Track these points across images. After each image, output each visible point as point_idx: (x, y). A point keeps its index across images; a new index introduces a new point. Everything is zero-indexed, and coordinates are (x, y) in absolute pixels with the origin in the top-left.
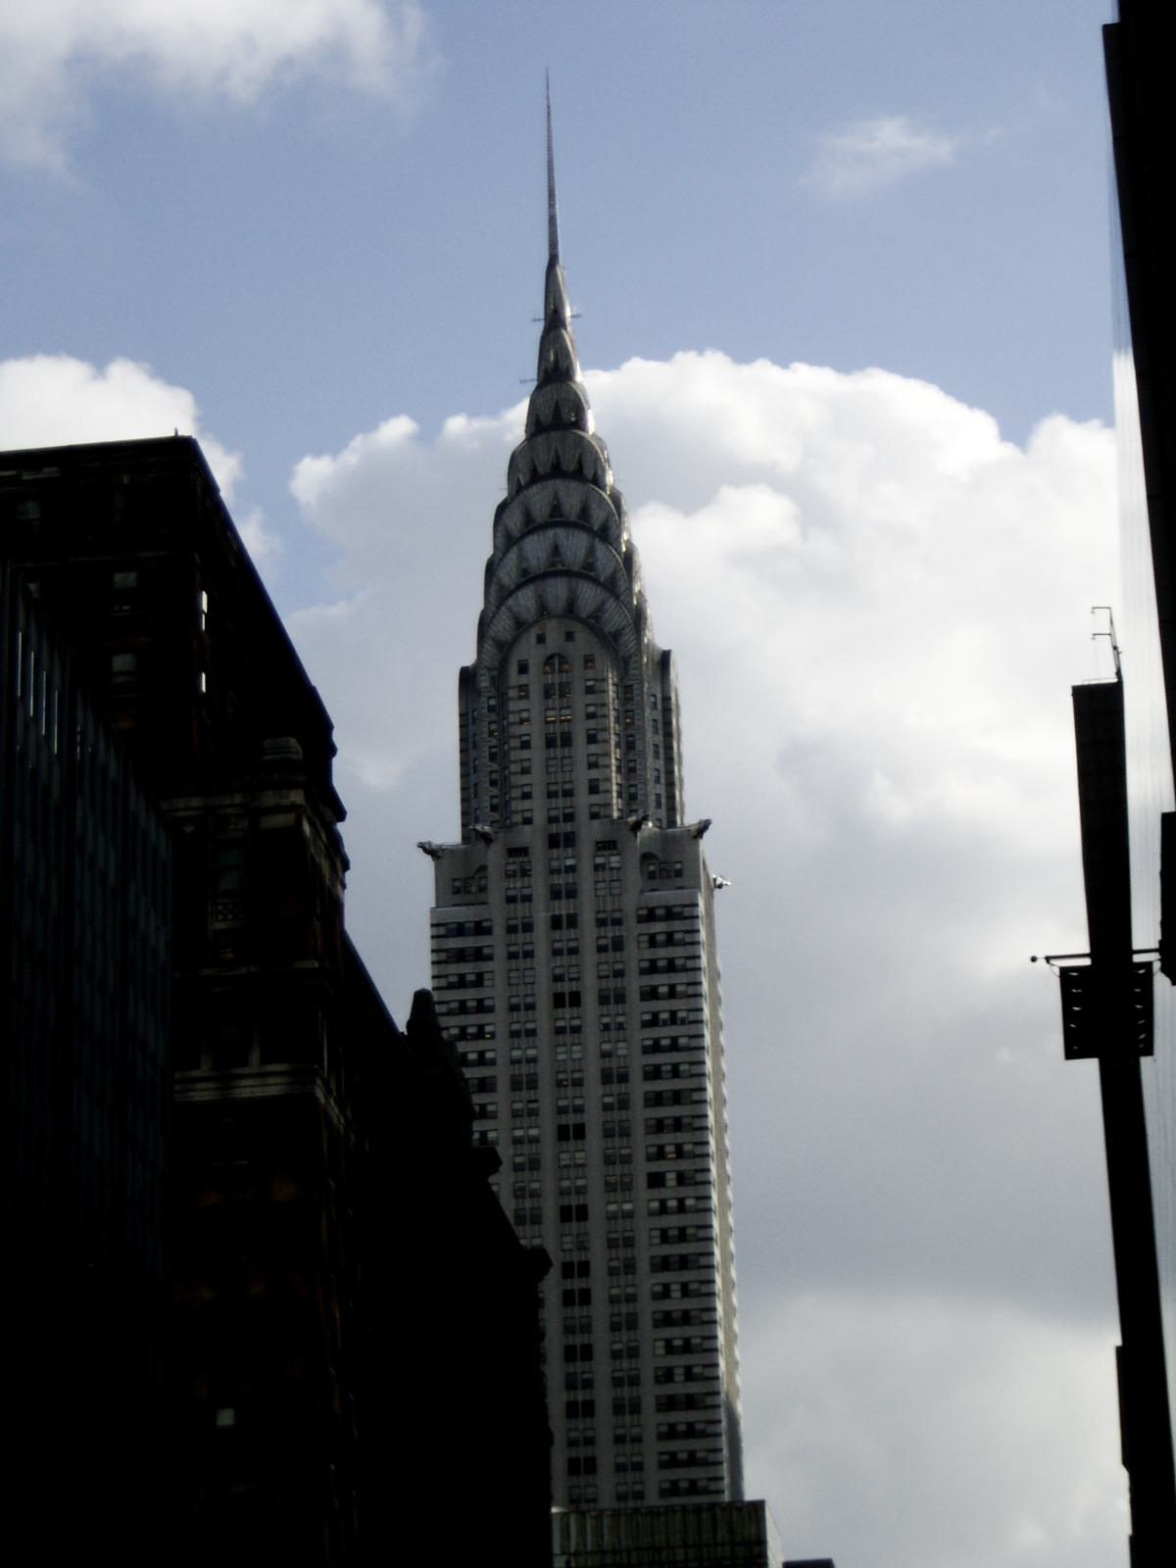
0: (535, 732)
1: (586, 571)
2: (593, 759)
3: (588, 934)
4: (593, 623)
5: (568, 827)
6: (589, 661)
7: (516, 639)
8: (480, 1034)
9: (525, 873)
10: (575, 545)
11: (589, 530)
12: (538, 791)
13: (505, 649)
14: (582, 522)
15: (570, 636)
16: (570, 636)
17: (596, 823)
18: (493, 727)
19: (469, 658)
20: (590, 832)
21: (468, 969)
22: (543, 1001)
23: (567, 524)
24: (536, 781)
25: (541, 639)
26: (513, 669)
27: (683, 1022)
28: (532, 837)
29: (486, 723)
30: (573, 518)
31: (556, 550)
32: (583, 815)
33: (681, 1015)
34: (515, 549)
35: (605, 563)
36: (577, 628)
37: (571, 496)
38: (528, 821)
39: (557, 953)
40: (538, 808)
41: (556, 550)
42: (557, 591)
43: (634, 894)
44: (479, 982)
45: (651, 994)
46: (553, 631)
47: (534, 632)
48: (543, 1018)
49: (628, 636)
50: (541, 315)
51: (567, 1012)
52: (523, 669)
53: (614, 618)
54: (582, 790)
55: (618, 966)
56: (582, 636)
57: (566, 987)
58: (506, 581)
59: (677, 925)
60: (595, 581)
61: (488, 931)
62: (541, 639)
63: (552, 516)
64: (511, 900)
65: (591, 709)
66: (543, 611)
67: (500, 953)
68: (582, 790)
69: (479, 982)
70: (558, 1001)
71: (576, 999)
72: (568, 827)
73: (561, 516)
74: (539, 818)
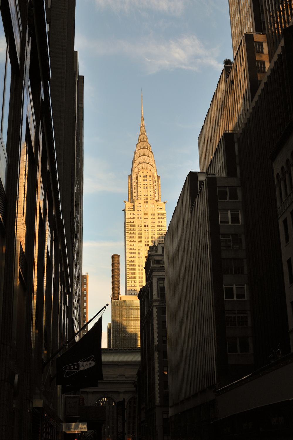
2: (150, 191)
3: (150, 217)
5: (147, 200)
6: (150, 176)
8: (133, 230)
9: (140, 206)
12: (143, 195)
15: (147, 172)
16: (147, 172)
17: (151, 200)
20: (150, 202)
21: (132, 220)
22: (143, 226)
24: (142, 193)
25: (143, 172)
26: (139, 176)
27: (163, 230)
28: (142, 201)
32: (149, 199)
33: (163, 229)
38: (141, 199)
39: (145, 219)
40: (143, 197)
42: (145, 165)
43: (156, 212)
44: (133, 222)
45: (159, 226)
47: (142, 171)
48: (143, 228)
51: (146, 227)
52: (140, 176)
54: (149, 195)
55: (154, 233)
57: (146, 224)
58: (137, 163)
59: (163, 216)
61: (135, 215)
62: (143, 172)
64: (138, 210)
66: (143, 168)
67: (136, 218)
68: (149, 195)
69: (133, 222)
70: (145, 226)
71: (148, 226)
72: (147, 200)
74: (143, 199)
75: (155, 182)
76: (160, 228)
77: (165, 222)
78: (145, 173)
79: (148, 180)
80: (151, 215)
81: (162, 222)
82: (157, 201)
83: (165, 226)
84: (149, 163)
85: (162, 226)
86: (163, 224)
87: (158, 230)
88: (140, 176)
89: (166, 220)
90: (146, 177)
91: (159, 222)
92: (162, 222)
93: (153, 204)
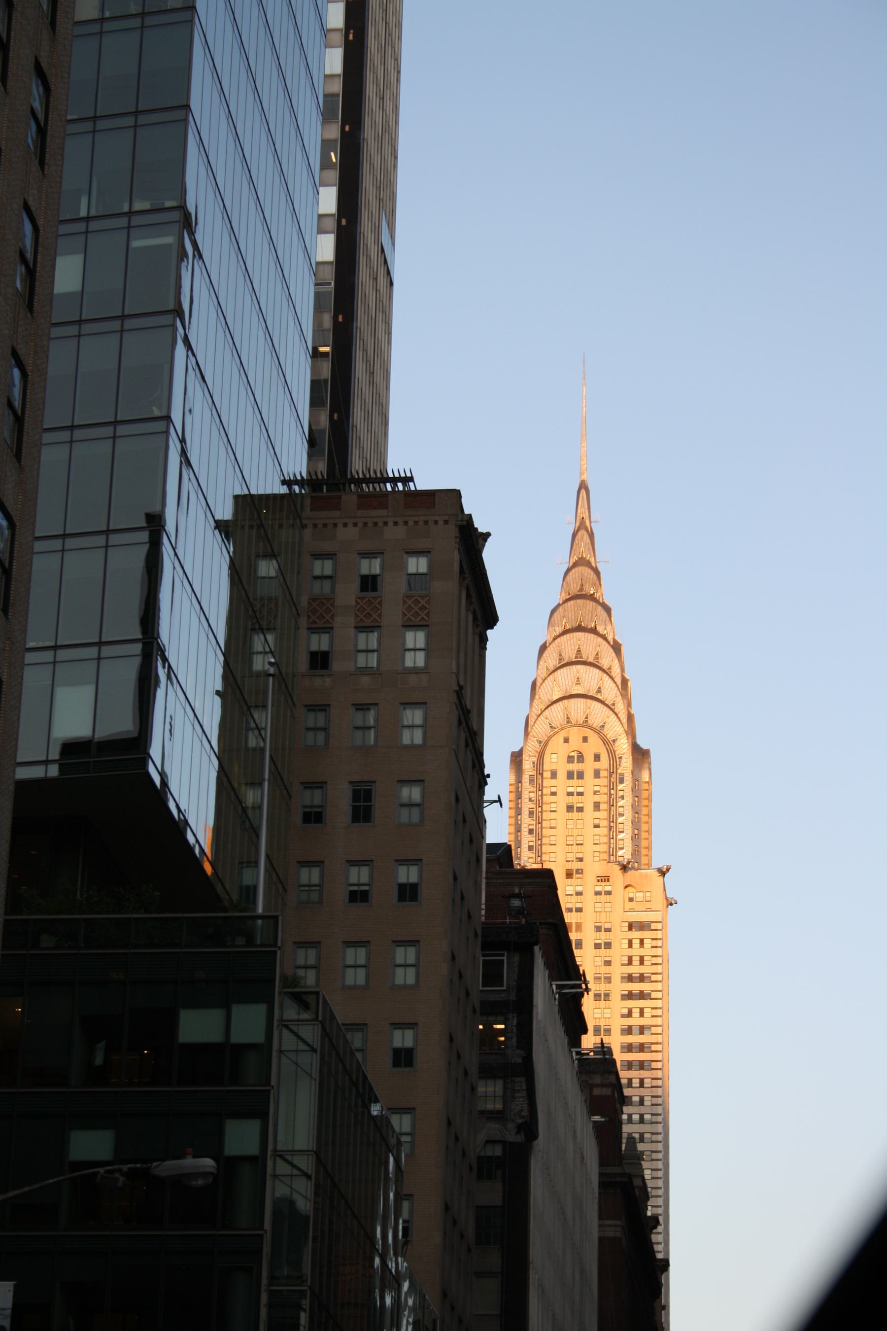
0: (562, 801)
6: (597, 757)
7: (550, 738)
10: (590, 678)
13: (544, 745)
15: (585, 739)
16: (585, 739)
18: (532, 795)
19: (517, 749)
23: (585, 663)
25: (566, 740)
29: (527, 793)
30: (591, 659)
37: (589, 644)
42: (577, 707)
46: (575, 735)
47: (563, 734)
56: (593, 737)
62: (566, 740)
63: (576, 657)
65: (597, 788)
72: (578, 865)
73: (582, 657)
75: (622, 781)
76: (636, 987)
77: (655, 960)
78: (576, 743)
79: (589, 774)
80: (598, 929)
81: (642, 962)
82: (624, 868)
83: (654, 978)
85: (642, 978)
86: (646, 969)
87: (623, 1016)
89: (659, 935)
90: (581, 758)
91: (630, 962)
92: (642, 962)
93: (605, 879)
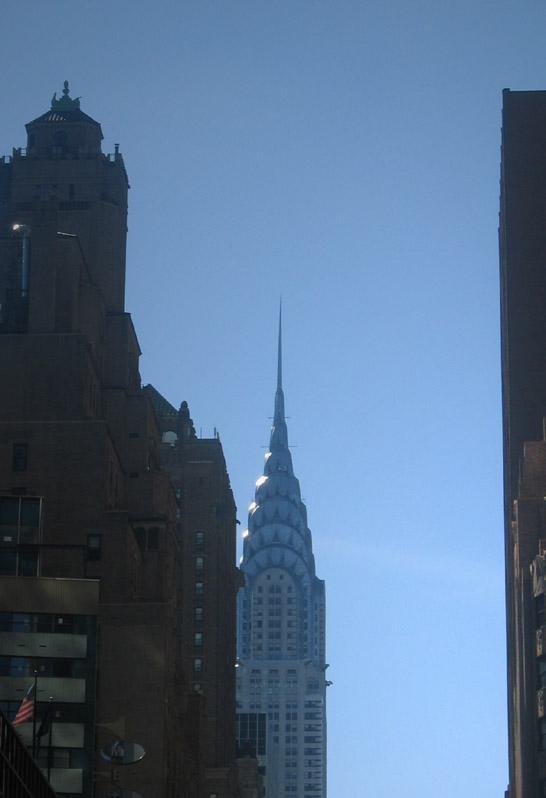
1: (289, 546)
4: (291, 570)
6: (290, 588)
10: (285, 532)
11: (292, 526)
14: (287, 522)
15: (281, 577)
23: (283, 522)
25: (269, 577)
31: (276, 536)
34: (257, 533)
35: (298, 542)
36: (284, 573)
41: (276, 536)
49: (306, 578)
50: (273, 415)
53: (301, 569)
60: (292, 549)
62: (269, 577)
84: (289, 546)
88: (260, 589)
